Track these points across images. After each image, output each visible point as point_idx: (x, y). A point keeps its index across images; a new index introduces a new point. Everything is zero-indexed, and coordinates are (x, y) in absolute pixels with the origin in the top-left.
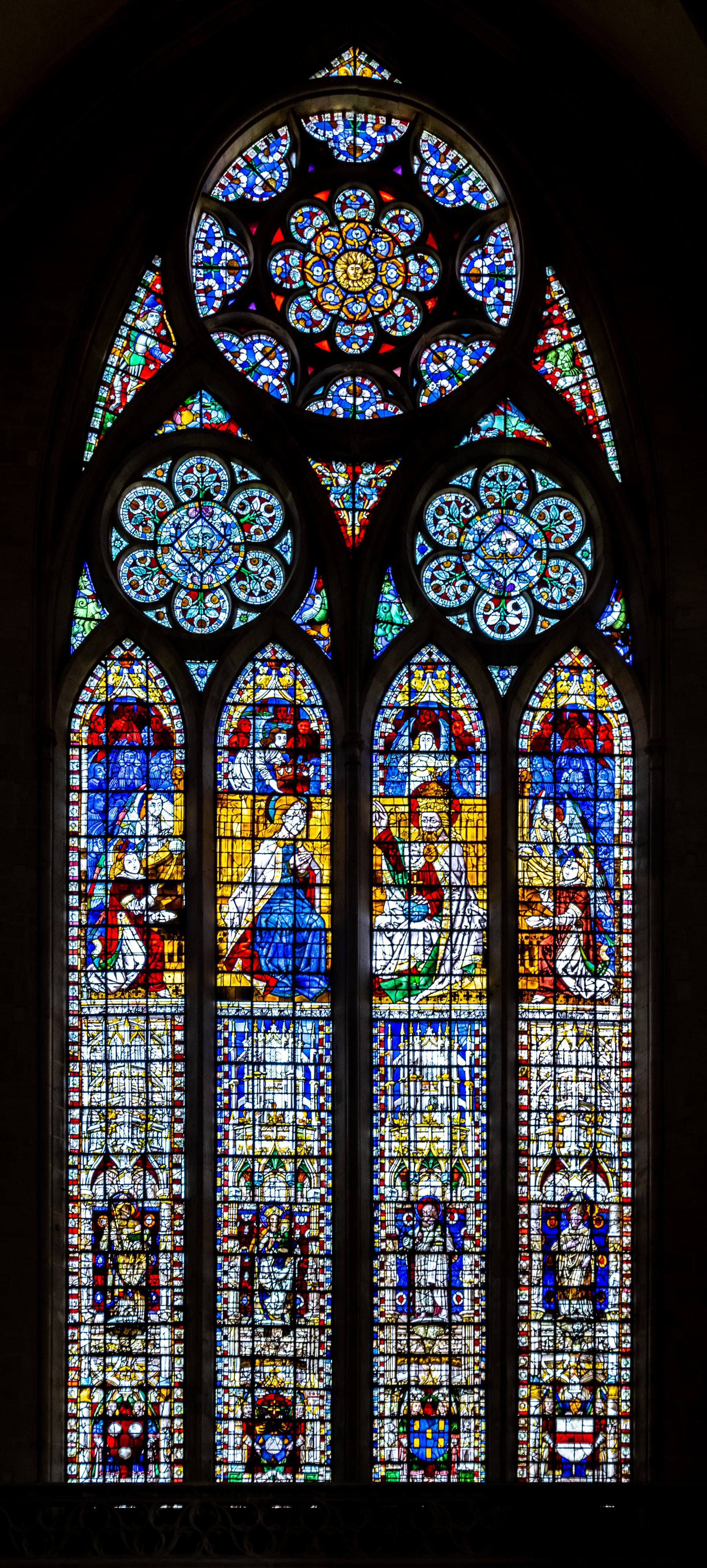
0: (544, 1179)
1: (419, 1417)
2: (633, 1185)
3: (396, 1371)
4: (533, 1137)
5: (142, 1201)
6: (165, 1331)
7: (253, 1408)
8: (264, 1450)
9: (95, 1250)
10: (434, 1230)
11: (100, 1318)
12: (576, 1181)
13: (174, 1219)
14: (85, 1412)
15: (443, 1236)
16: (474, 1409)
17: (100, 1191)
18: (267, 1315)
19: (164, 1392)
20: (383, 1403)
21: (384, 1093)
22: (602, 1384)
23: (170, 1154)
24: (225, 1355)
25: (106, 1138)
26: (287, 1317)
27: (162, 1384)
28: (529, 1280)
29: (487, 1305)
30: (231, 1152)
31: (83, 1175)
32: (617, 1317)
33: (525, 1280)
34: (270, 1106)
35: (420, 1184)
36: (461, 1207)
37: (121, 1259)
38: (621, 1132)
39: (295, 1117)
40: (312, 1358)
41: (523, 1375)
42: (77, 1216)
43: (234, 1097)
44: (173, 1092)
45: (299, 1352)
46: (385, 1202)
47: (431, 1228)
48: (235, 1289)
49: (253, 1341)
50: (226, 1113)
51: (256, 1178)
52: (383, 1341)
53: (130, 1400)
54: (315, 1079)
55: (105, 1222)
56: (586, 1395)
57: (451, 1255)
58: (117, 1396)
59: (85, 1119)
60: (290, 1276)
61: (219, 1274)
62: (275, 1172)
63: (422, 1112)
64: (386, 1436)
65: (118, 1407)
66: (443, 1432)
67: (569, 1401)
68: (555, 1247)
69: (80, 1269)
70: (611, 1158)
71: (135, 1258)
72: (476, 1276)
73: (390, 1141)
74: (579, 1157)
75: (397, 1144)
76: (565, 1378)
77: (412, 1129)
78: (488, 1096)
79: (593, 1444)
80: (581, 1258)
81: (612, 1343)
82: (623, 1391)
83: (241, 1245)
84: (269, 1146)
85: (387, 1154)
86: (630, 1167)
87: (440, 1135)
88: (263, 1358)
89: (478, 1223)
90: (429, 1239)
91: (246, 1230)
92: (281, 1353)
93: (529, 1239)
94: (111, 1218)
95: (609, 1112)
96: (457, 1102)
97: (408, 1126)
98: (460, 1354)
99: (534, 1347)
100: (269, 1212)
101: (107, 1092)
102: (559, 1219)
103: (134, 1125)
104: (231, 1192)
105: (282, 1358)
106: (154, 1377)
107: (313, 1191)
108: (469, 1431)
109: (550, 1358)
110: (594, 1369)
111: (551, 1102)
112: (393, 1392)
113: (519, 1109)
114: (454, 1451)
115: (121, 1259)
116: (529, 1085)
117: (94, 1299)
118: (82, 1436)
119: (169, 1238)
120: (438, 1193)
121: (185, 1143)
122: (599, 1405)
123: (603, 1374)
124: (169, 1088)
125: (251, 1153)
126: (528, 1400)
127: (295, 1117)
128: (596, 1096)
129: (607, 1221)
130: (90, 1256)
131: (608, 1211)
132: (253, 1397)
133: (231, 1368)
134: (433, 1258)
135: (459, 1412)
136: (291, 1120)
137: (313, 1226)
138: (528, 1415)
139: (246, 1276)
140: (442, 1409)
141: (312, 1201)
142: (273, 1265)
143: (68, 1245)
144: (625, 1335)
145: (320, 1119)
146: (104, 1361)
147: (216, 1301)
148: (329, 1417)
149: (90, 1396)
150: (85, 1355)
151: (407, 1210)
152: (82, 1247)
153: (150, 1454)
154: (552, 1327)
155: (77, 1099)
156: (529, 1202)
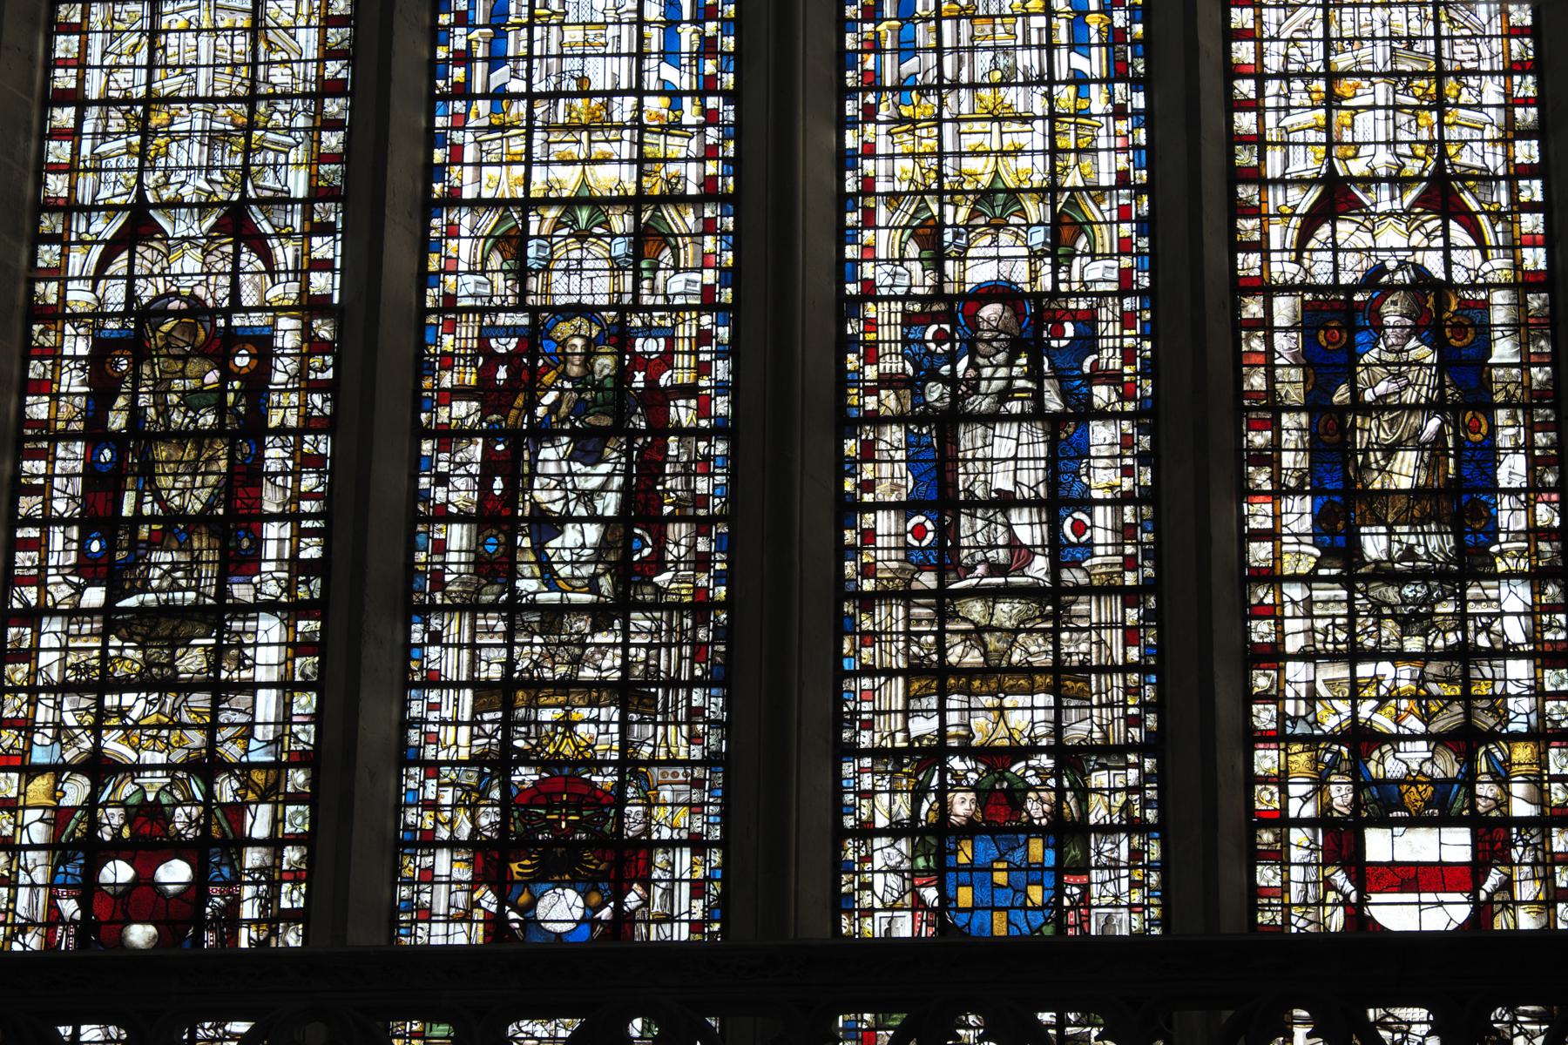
0: (1306, 233)
1: (970, 829)
2: (1549, 241)
3: (907, 713)
4: (1272, 135)
5: (227, 314)
6: (270, 628)
7: (505, 815)
8: (531, 922)
9: (95, 434)
10: (1010, 364)
11: (94, 597)
12: (1391, 236)
13: (311, 354)
14: (38, 833)
15: (1035, 374)
16: (1128, 803)
17: (115, 294)
18: (549, 577)
19: (258, 777)
20: (871, 794)
21: (876, 48)
22: (1492, 736)
23: (308, 203)
24: (434, 681)
25: (141, 170)
26: (605, 583)
27: (254, 757)
28: (1275, 478)
29: (1157, 542)
30: (468, 193)
31: (76, 258)
32: (1523, 565)
33: (1262, 479)
34: (573, 87)
35: (971, 253)
36: (1083, 305)
37: (162, 453)
38: (1510, 119)
39: (640, 107)
40: (673, 683)
41: (1264, 716)
42: (55, 354)
43: (480, 69)
44: (321, 61)
45: (638, 671)
46: (877, 300)
47: (1001, 357)
48: (462, 518)
49: (510, 645)
50: (459, 106)
51: (531, 252)
52: (871, 637)
53: (165, 799)
54: (692, 22)
55: (124, 365)
56: (1447, 766)
57: (1054, 424)
58: (127, 789)
59: (88, 127)
60: (617, 481)
61: (424, 482)
62: (582, 237)
63: (973, 86)
64: (879, 881)
65: (128, 819)
66: (1042, 868)
67: (1398, 782)
68: (1342, 395)
69: (49, 477)
70: (1486, 178)
71: (199, 448)
72: (1127, 471)
73: (892, 156)
74: (1398, 181)
75: (908, 164)
76: (1384, 722)
77: (948, 128)
78: (1147, 45)
79: (1475, 892)
80: (1415, 421)
81: (1515, 631)
82: (1553, 752)
83: (485, 412)
84: (568, 179)
85: (881, 187)
86: (1538, 197)
87: (1024, 140)
88: (536, 686)
89: (1128, 342)
90: (997, 385)
91: (502, 374)
92: (588, 673)
93: (1271, 378)
94: (139, 350)
95: (1476, 72)
96: (1065, 61)
97: (939, 121)
98: (1085, 668)
99: (1293, 644)
100: (564, 329)
101: (151, 67)
102: (1353, 330)
103: (214, 139)
104: (466, 287)
105: (589, 685)
106: (234, 739)
107: (683, 277)
108: (1114, 865)
109: (1340, 672)
110: (1467, 698)
111: (1319, 52)
112: (899, 766)
113: (1233, 72)
114: (1071, 918)
115: (162, 453)
116: (1258, 18)
117: (83, 550)
118: (23, 894)
119: (294, 398)
120: (1021, 273)
121: (345, 177)
122: (1486, 790)
123: (1493, 709)
124: (311, 52)
125: (520, 193)
126: (1282, 780)
127: (640, 107)
128: (1438, 38)
129: (1485, 328)
130: (79, 447)
131: (1486, 305)
132: (506, 786)
133: (447, 714)
134: (1011, 429)
135: (1085, 814)
136: (627, 117)
137: (681, 361)
138: (1282, 821)
139: (498, 484)
140: (1036, 809)
141: (679, 301)
142: (571, 458)
143: (22, 420)
144: (1552, 609)
145: (704, 111)
146: (100, 703)
147: (412, 548)
148: (716, 833)
149: (56, 792)
150: (49, 688)
151: (936, 318)
152: (60, 425)
153: (210, 938)
154: (1343, 594)
155: (72, 84)
156: (1267, 289)
